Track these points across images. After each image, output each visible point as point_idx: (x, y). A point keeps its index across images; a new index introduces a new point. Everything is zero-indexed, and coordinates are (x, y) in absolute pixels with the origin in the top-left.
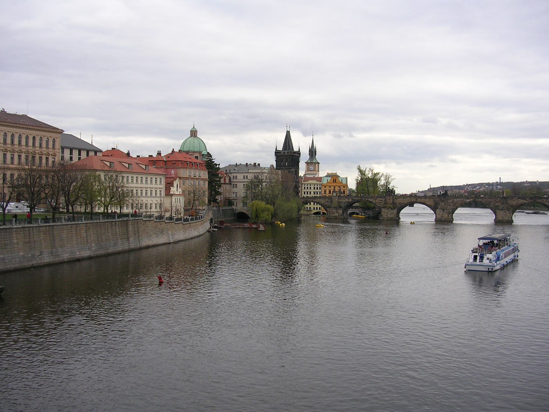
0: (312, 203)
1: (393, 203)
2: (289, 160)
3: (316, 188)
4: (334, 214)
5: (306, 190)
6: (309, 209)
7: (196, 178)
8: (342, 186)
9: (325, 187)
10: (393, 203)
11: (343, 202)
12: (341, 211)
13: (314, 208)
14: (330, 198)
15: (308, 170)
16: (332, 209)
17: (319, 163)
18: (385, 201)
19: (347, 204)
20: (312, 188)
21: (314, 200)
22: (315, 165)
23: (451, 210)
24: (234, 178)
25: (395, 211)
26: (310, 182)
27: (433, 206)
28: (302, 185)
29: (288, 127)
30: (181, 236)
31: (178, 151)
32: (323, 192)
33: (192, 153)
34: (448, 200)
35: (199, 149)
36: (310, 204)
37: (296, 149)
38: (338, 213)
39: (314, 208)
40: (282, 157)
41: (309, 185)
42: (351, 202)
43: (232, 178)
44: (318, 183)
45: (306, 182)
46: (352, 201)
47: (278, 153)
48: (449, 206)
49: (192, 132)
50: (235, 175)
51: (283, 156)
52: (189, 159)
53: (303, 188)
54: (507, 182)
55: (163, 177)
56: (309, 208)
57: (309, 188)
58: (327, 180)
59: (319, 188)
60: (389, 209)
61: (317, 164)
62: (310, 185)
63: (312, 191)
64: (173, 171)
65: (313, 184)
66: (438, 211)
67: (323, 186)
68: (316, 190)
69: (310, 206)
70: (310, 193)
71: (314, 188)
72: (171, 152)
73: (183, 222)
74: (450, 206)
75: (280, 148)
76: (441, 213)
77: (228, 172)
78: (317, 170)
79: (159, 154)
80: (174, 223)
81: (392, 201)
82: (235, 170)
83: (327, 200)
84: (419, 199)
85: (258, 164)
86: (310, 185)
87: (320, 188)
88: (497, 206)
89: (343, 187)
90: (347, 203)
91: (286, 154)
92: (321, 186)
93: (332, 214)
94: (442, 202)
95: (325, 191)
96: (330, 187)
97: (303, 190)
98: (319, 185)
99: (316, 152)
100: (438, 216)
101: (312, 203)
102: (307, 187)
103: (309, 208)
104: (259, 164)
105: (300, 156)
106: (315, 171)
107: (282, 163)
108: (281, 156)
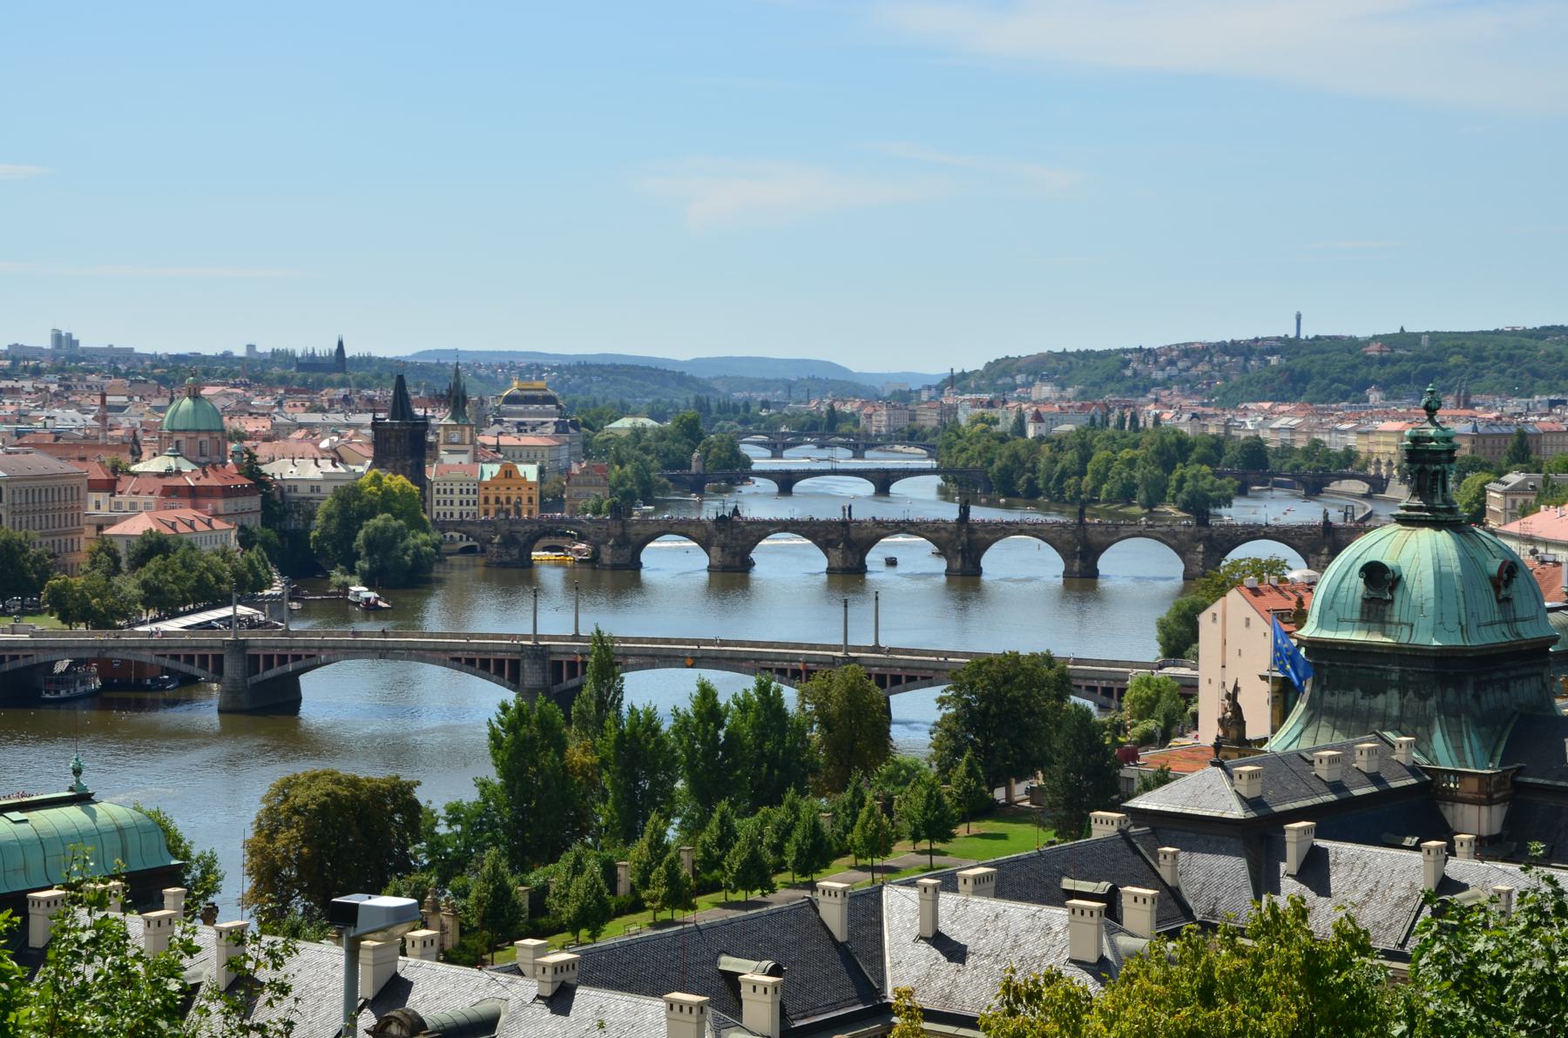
1: (623, 534)
9: (486, 488)
10: (623, 534)
12: (515, 552)
20: (456, 491)
21: (459, 525)
22: (463, 430)
24: (290, 490)
25: (627, 552)
32: (482, 500)
34: (732, 528)
38: (511, 555)
41: (448, 484)
43: (286, 490)
50: (293, 484)
53: (435, 491)
54: (1317, 338)
57: (448, 491)
59: (471, 492)
61: (467, 429)
63: (456, 497)
65: (456, 481)
66: (713, 549)
68: (465, 497)
71: (461, 491)
74: (736, 539)
81: (618, 531)
83: (486, 528)
84: (675, 526)
87: (474, 490)
88: (831, 540)
91: (397, 427)
96: (498, 489)
100: (713, 561)
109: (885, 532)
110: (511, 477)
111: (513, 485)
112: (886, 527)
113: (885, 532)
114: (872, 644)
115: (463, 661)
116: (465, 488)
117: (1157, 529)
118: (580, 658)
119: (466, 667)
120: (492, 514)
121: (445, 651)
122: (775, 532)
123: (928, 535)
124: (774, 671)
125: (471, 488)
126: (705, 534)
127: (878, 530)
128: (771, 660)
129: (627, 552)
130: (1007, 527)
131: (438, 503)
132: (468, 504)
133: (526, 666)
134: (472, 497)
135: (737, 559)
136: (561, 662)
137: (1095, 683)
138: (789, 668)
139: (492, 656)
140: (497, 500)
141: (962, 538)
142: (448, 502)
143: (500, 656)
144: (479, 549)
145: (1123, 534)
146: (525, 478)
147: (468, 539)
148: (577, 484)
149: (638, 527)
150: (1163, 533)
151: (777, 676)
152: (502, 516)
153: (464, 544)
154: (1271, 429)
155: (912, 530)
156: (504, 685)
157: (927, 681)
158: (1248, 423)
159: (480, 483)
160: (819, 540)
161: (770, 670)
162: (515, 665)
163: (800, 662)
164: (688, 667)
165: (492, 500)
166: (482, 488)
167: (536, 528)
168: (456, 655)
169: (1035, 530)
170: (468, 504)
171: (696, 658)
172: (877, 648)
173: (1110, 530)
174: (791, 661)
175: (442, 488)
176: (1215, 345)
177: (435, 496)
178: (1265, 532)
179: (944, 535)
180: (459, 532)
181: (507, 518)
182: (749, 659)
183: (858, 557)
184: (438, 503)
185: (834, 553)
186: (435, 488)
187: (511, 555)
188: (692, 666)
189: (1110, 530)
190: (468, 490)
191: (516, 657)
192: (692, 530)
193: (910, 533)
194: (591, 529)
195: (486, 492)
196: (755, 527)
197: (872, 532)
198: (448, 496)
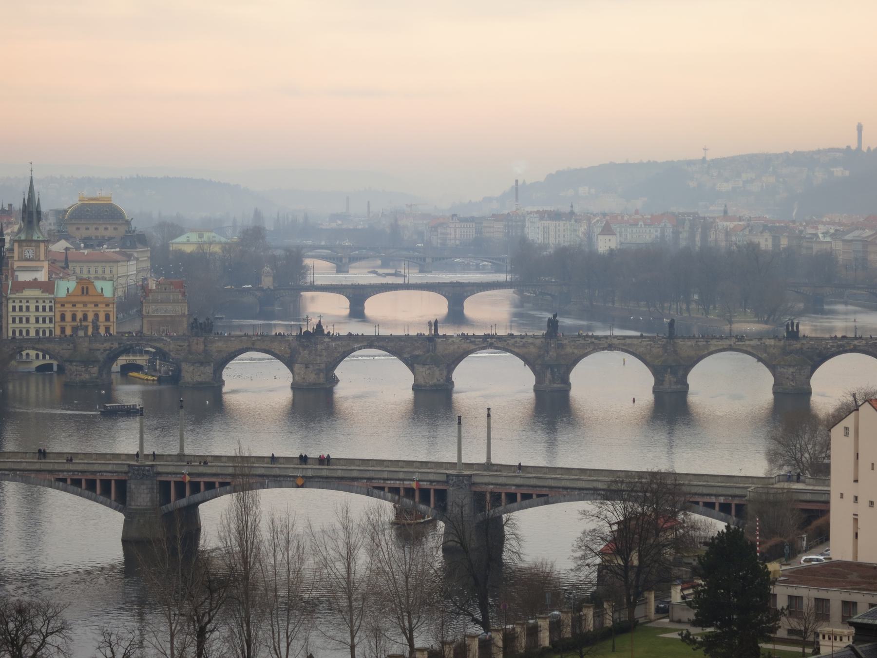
3: (41, 309)
9: (63, 305)
11: (99, 350)
12: (95, 370)
14: (72, 340)
16: (76, 366)
18: (189, 346)
20: (32, 308)
21: (36, 343)
23: (323, 366)
25: (209, 370)
26: (28, 293)
27: (287, 356)
34: (316, 344)
44: (46, 295)
45: (18, 295)
46: (120, 347)
48: (318, 358)
53: (10, 309)
57: (24, 309)
58: (68, 289)
59: (47, 309)
60: (197, 365)
62: (28, 302)
65: (31, 298)
66: (297, 367)
67: (59, 303)
71: (37, 308)
74: (320, 356)
76: (303, 373)
78: (42, 257)
81: (201, 347)
86: (28, 302)
87: (51, 308)
88: (418, 356)
89: (104, 305)
90: (107, 352)
92: (52, 304)
93: (76, 375)
94: (305, 350)
97: (10, 314)
98: (48, 301)
100: (297, 378)
102: (21, 308)
106: (39, 260)
109: (472, 347)
110: (87, 293)
112: (473, 342)
113: (472, 347)
114: (483, 460)
115: (69, 481)
117: (747, 343)
118: (188, 478)
119: (71, 488)
120: (68, 332)
121: (51, 472)
122: (360, 348)
123: (516, 350)
124: (386, 490)
126: (289, 351)
127: (465, 346)
128: (385, 479)
129: (209, 370)
130: (596, 341)
131: (14, 321)
132: (44, 321)
133: (133, 486)
134: (48, 314)
135: (322, 375)
136: (169, 482)
137: (713, 499)
138: (402, 486)
139: (98, 477)
140: (74, 318)
141: (551, 353)
142: (24, 320)
143: (106, 476)
144: (55, 368)
145: (712, 348)
146: (101, 295)
147: (44, 357)
148: (155, 301)
149: (220, 344)
150: (753, 347)
151: (389, 495)
154: (844, 241)
155: (500, 345)
156: (110, 506)
157: (542, 499)
158: (820, 235)
159: (55, 300)
160: (406, 356)
161: (382, 489)
162: (122, 486)
163: (413, 480)
164: (298, 487)
165: (68, 317)
166: (59, 305)
167: (116, 345)
168: (61, 476)
169: (624, 345)
170: (44, 321)
171: (306, 477)
172: (488, 466)
173: (700, 344)
174: (404, 480)
176: (777, 156)
177: (11, 314)
178: (855, 346)
179: (533, 350)
180: (34, 348)
181: (86, 333)
182: (362, 478)
183: (445, 373)
184: (14, 321)
185: (421, 370)
188: (302, 486)
189: (700, 344)
190: (44, 308)
191: (123, 477)
192: (275, 347)
193: (496, 348)
194: (172, 346)
196: (339, 343)
197: (458, 347)
198: (24, 313)
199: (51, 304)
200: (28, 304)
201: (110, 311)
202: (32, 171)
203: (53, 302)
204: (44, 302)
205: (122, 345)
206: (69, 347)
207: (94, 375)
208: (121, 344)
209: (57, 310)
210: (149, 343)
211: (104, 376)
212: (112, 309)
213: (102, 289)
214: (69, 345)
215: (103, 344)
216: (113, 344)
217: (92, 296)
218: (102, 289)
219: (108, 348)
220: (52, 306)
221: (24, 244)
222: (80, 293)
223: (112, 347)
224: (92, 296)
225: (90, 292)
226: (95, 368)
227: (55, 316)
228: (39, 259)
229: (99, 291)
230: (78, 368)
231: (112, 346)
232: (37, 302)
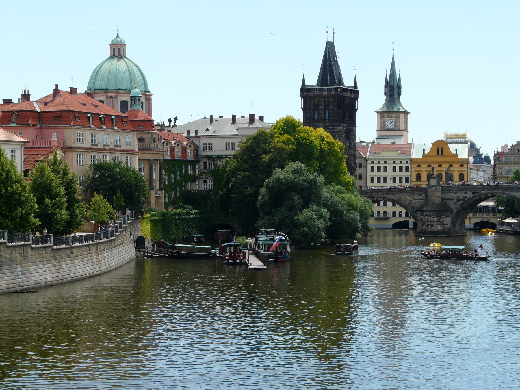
0: (389, 204)
2: (331, 107)
3: (398, 169)
4: (432, 225)
5: (376, 173)
6: (382, 214)
7: (110, 150)
8: (435, 163)
9: (419, 166)
11: (452, 200)
12: (448, 221)
13: (394, 213)
15: (382, 128)
16: (428, 215)
17: (406, 113)
19: (461, 205)
20: (390, 169)
22: (398, 117)
24: (205, 149)
28: (366, 161)
29: (330, 34)
30: (48, 276)
31: (69, 90)
32: (414, 178)
33: (113, 95)
35: (129, 84)
36: (385, 204)
37: (348, 83)
38: (442, 224)
39: (394, 213)
40: (316, 100)
41: (382, 162)
42: (470, 198)
43: (201, 148)
46: (474, 197)
47: (309, 90)
49: (114, 47)
50: (208, 141)
51: (318, 96)
52: (94, 107)
53: (369, 169)
55: (19, 147)
56: (382, 212)
57: (382, 169)
58: (424, 150)
59: (404, 169)
61: (402, 116)
64: (54, 134)
67: (414, 164)
68: (398, 174)
69: (385, 209)
70: (385, 180)
71: (394, 169)
72: (52, 92)
73: (52, 244)
75: (312, 81)
77: (192, 135)
78: (402, 127)
79: (26, 97)
80: (29, 247)
82: (207, 130)
85: (259, 116)
86: (385, 162)
87: (407, 169)
89: (458, 166)
90: (461, 202)
91: (325, 94)
92: (409, 165)
93: (428, 226)
95: (419, 177)
97: (368, 174)
98: (404, 162)
99: (399, 87)
101: (389, 204)
102: (379, 169)
103: (382, 212)
104: (261, 118)
105: (357, 98)
106: (399, 130)
107: (317, 112)
108: (314, 97)
110: (442, 154)
111: (445, 163)
116: (398, 166)
125: (404, 166)
131: (372, 180)
134: (405, 174)
142: (382, 180)
144: (411, 225)
146: (456, 155)
148: (508, 163)
152: (433, 182)
153: (397, 220)
159: (412, 160)
166: (416, 166)
167: (469, 195)
175: (376, 166)
177: (370, 174)
184: (372, 180)
186: (369, 166)
187: (442, 224)
190: (401, 169)
195: (419, 169)
198: (382, 174)
199: (407, 165)
200: (385, 165)
201: (465, 171)
202: (393, 49)
203: (409, 162)
204: (401, 162)
205: (477, 194)
206: (421, 197)
207: (446, 226)
208: (475, 193)
209: (413, 170)
210: (505, 192)
211: (457, 228)
212: (466, 169)
213: (456, 150)
214: (420, 195)
215: (456, 194)
216: (466, 193)
217: (447, 156)
218: (456, 150)
219: (462, 198)
220: (408, 167)
221: (386, 115)
222: (436, 153)
223: (466, 197)
224: (447, 156)
225: (445, 153)
226: (448, 219)
227: (411, 176)
228: (400, 129)
229: (454, 153)
230: (429, 218)
231: (466, 195)
232: (394, 162)
